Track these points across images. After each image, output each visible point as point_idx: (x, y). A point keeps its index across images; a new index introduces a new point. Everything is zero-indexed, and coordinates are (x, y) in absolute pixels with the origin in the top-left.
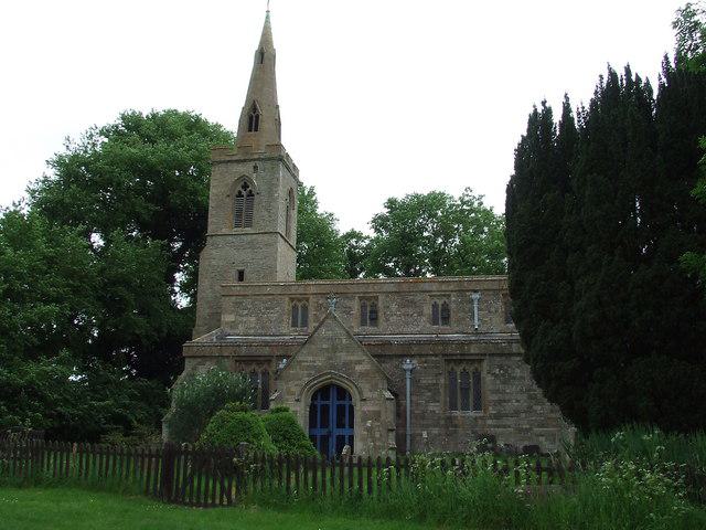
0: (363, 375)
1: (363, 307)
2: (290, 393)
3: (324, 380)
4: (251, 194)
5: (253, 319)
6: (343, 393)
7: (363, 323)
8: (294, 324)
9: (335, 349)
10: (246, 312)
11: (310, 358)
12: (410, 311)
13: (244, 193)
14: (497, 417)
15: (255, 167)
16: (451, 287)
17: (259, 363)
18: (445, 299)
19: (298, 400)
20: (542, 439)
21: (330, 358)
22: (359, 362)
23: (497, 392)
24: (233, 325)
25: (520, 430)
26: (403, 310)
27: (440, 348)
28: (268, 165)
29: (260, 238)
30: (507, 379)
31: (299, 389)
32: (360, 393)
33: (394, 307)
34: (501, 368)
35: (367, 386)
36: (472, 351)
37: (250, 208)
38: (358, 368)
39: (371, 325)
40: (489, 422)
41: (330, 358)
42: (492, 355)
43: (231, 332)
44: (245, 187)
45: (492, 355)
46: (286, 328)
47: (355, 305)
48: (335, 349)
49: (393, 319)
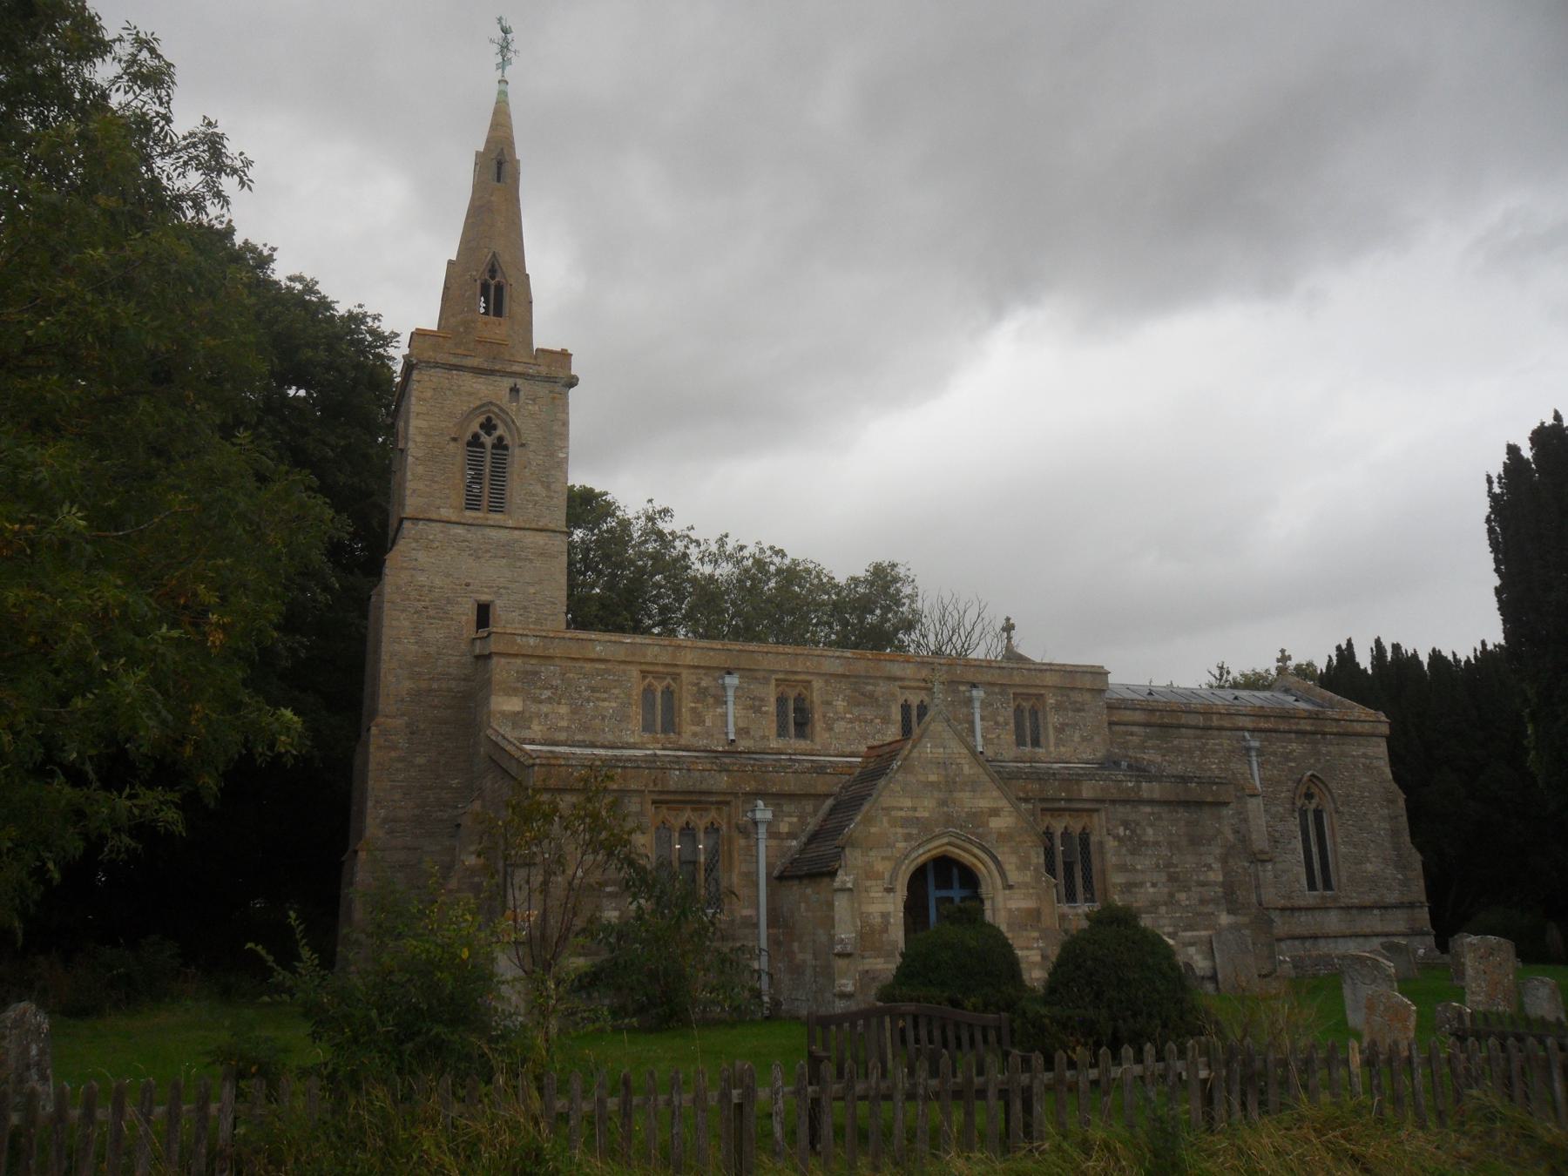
0: (1003, 837)
1: (781, 701)
2: (871, 874)
3: (922, 855)
4: (500, 444)
5: (563, 710)
6: (970, 879)
7: (782, 732)
8: (648, 727)
9: (950, 785)
10: (547, 693)
11: (908, 803)
12: (869, 713)
13: (487, 440)
15: (514, 390)
18: (923, 695)
19: (889, 890)
20: (1192, 950)
22: (995, 812)
23: (1123, 868)
24: (518, 719)
26: (856, 711)
27: (1036, 786)
28: (542, 390)
29: (531, 539)
30: (1135, 845)
31: (889, 865)
33: (840, 704)
34: (1126, 824)
36: (1085, 795)
38: (996, 823)
42: (1113, 802)
44: (488, 426)
45: (1113, 802)
46: (633, 731)
47: (771, 694)
49: (840, 726)
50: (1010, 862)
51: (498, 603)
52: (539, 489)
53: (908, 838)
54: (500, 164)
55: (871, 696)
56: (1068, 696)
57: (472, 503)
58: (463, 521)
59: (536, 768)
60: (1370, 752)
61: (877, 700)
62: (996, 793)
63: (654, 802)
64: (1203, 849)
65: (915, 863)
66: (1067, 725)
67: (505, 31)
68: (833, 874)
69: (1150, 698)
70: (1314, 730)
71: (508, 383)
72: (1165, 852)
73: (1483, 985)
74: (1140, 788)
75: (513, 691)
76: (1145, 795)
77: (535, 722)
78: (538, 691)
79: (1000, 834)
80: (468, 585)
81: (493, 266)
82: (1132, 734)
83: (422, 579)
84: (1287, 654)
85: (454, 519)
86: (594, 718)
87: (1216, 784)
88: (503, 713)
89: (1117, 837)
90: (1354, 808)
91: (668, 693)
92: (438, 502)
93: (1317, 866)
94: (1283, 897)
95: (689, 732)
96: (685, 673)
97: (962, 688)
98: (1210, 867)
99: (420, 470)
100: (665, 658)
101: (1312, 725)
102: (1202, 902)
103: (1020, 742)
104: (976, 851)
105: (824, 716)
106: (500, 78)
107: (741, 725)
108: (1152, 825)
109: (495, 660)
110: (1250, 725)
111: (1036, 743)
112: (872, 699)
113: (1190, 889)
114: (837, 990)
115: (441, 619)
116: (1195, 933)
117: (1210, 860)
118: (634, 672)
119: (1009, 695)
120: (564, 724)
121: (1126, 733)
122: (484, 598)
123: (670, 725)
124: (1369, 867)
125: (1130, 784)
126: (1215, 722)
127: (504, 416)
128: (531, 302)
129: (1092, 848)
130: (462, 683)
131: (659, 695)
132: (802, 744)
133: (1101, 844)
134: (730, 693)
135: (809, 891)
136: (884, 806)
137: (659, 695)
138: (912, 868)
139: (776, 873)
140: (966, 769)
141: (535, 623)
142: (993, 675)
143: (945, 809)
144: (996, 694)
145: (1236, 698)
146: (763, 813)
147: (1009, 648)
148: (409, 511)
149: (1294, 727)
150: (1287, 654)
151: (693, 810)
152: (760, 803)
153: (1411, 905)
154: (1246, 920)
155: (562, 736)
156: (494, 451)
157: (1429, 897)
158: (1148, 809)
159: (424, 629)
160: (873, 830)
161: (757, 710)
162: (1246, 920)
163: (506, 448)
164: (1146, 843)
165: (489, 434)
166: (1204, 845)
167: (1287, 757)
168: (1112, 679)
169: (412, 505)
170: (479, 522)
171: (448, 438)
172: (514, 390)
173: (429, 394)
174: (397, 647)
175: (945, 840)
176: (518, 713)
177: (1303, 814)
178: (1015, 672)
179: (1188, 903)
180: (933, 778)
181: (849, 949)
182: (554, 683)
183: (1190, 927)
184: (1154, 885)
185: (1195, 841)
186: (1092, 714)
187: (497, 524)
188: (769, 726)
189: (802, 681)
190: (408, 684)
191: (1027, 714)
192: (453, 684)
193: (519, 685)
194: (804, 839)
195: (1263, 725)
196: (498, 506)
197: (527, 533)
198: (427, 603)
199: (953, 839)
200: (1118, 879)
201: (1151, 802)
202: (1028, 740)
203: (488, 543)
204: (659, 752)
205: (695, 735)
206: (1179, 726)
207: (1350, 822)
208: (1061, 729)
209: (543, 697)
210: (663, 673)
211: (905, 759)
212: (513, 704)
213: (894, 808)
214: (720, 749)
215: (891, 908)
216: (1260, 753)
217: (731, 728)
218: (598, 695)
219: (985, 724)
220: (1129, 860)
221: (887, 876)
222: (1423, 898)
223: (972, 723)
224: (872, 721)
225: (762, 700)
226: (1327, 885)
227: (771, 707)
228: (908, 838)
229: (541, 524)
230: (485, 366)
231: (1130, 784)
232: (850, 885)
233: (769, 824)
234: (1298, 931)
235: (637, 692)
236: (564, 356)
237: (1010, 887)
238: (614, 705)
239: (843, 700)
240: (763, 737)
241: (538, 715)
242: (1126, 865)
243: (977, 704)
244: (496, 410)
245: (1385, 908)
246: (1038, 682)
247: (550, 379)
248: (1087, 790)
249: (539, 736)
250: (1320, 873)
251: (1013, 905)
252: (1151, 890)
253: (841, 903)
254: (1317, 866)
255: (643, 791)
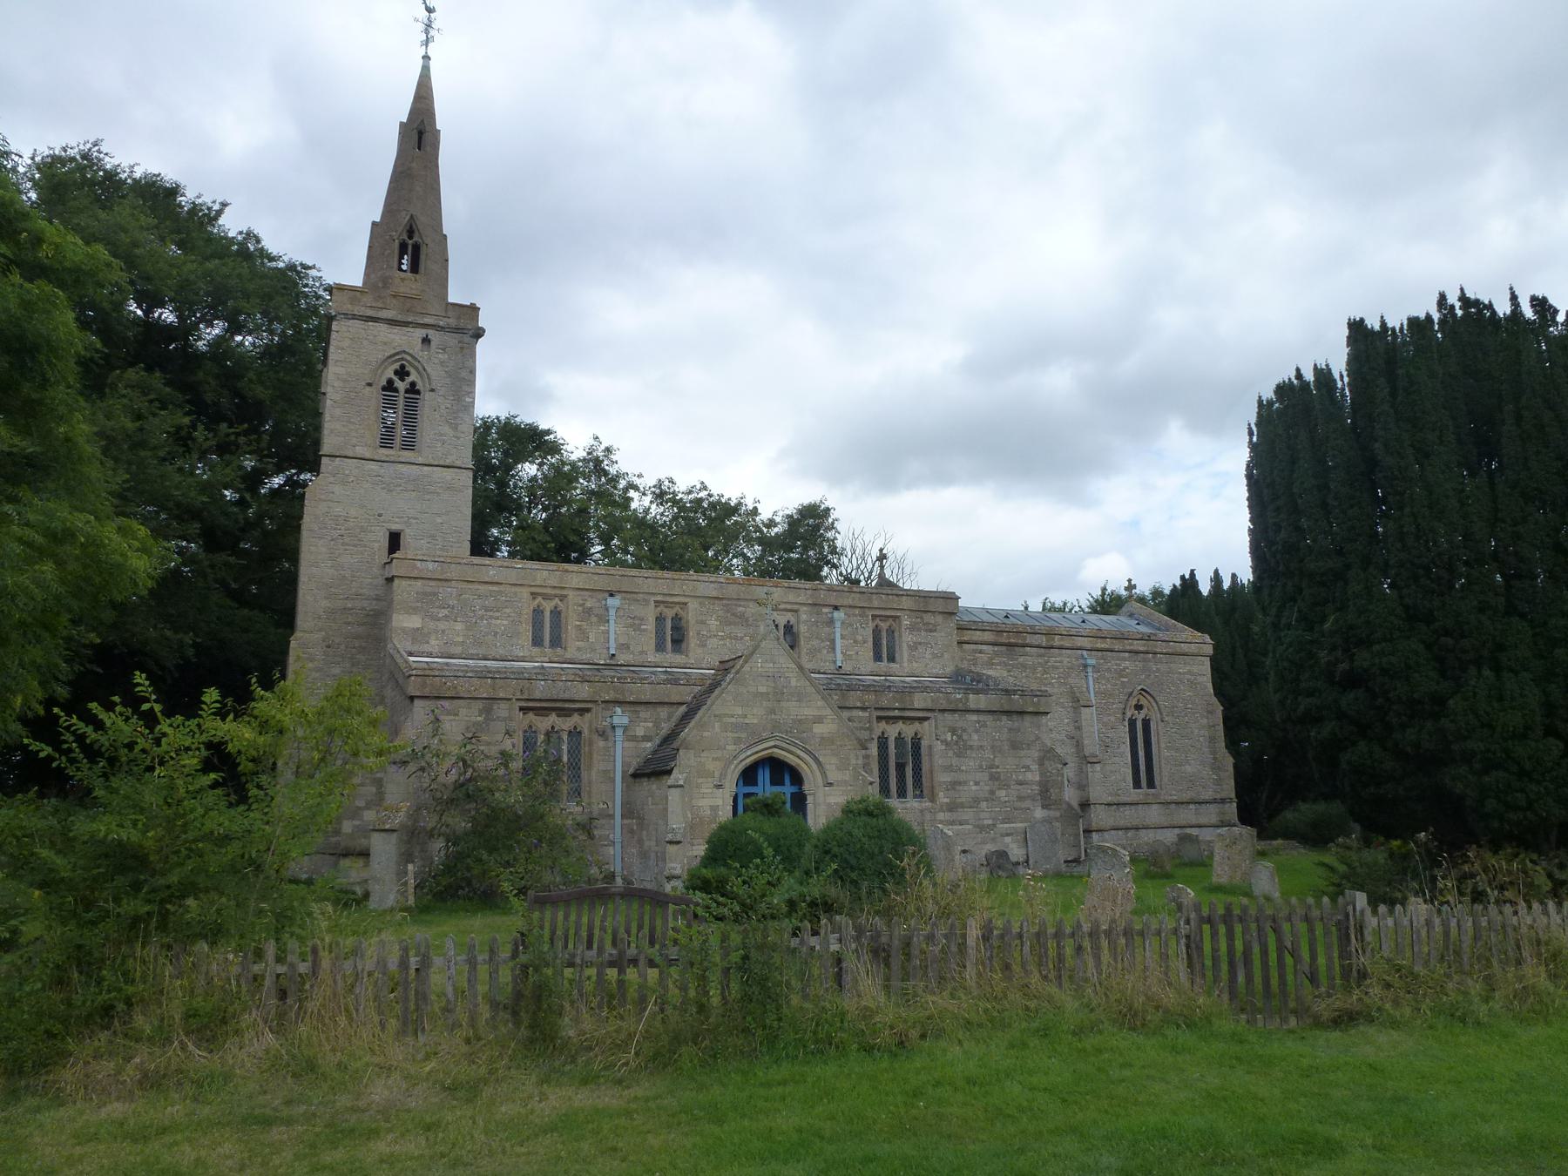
0: (826, 741)
1: (660, 619)
4: (413, 389)
7: (660, 647)
8: (537, 641)
9: (778, 695)
11: (739, 711)
13: (401, 386)
14: (952, 807)
15: (426, 341)
16: (801, 599)
17: (564, 713)
18: (790, 616)
19: (719, 787)
20: (1008, 840)
21: (773, 711)
22: (819, 720)
23: (948, 769)
24: (418, 635)
25: (982, 828)
26: (727, 629)
32: (824, 774)
33: (713, 623)
34: (953, 731)
35: (834, 760)
37: (411, 416)
38: (818, 729)
39: (674, 651)
40: (941, 816)
41: (773, 711)
42: (943, 711)
43: (415, 648)
44: (402, 373)
45: (943, 711)
46: (523, 645)
47: (650, 614)
48: (778, 695)
50: (831, 763)
51: (407, 531)
52: (447, 429)
53: (737, 741)
54: (421, 134)
55: (742, 616)
56: (922, 618)
57: (386, 441)
58: (376, 458)
59: (413, 678)
60: (1195, 669)
61: (747, 620)
62: (820, 703)
63: (521, 709)
64: (1022, 753)
65: (744, 763)
66: (920, 644)
67: (430, 10)
68: (669, 772)
69: (1006, 621)
70: (1145, 650)
71: (420, 333)
72: (988, 755)
73: (1226, 868)
74: (967, 699)
75: (415, 610)
76: (972, 706)
77: (433, 637)
78: (435, 610)
79: (822, 738)
80: (380, 515)
81: (411, 227)
82: (981, 652)
83: (338, 509)
84: (1133, 583)
85: (368, 455)
86: (487, 634)
87: (1036, 696)
88: (404, 630)
89: (945, 742)
90: (1178, 717)
91: (556, 613)
92: (354, 441)
93: (1143, 768)
94: (1110, 794)
95: (574, 647)
96: (571, 594)
97: (825, 610)
98: (1028, 768)
99: (338, 412)
100: (553, 582)
101: (1144, 646)
102: (1021, 798)
103: (878, 657)
104: (799, 752)
105: (698, 634)
106: (424, 53)
107: (621, 641)
108: (977, 731)
109: (396, 581)
110: (1089, 646)
111: (892, 659)
112: (743, 620)
113: (1009, 786)
114: (666, 873)
115: (355, 546)
116: (1012, 825)
117: (1028, 762)
118: (525, 593)
119: (867, 616)
120: (460, 639)
121: (975, 651)
122: (395, 527)
123: (556, 642)
124: (1188, 769)
125: (958, 696)
126: (1057, 641)
127: (416, 364)
128: (447, 260)
129: (924, 751)
130: (374, 602)
131: (547, 614)
132: (679, 659)
133: (930, 747)
134: (612, 612)
135: (654, 787)
136: (717, 713)
137: (547, 614)
138: (741, 767)
139: (631, 771)
140: (794, 682)
141: (441, 550)
142: (854, 599)
143: (773, 716)
144: (856, 616)
145: (1083, 622)
146: (620, 717)
147: (881, 576)
148: (325, 449)
149: (1128, 648)
150: (1133, 583)
151: (558, 716)
152: (619, 710)
153: (1223, 801)
154: (1058, 814)
155: (458, 650)
156: (407, 395)
157: (1237, 795)
158: (974, 717)
159: (339, 554)
160: (706, 734)
161: (637, 628)
162: (1058, 814)
163: (418, 392)
164: (971, 747)
165: (403, 380)
166: (1023, 749)
167: (1121, 673)
168: (961, 603)
169: (328, 444)
170: (392, 459)
171: (364, 383)
172: (426, 341)
173: (347, 343)
174: (314, 570)
175: (772, 743)
176: (418, 629)
177: (1132, 723)
178: (874, 597)
179: (1006, 799)
180: (762, 689)
181: (678, 838)
182: (451, 603)
183: (1007, 820)
184: (976, 783)
185: (1015, 746)
186: (943, 634)
187: (407, 460)
188: (650, 641)
189: (679, 603)
190: (325, 603)
191: (884, 634)
192: (365, 604)
193: (419, 604)
194: (657, 741)
195: (1100, 645)
196: (409, 445)
197: (435, 469)
198: (342, 532)
199: (778, 743)
200: (943, 778)
201: (978, 711)
202: (885, 656)
203: (400, 478)
204: (545, 665)
205: (579, 649)
206: (1024, 646)
207: (1173, 730)
208: (914, 647)
209: (440, 615)
210: (551, 595)
211: (737, 672)
212: (414, 622)
213: (725, 715)
214: (602, 662)
215: (720, 802)
216: (1096, 669)
217: (612, 644)
218: (491, 613)
219: (846, 642)
220: (955, 761)
221: (717, 774)
222: (1233, 795)
223: (833, 641)
224: (742, 638)
225: (642, 619)
226: (1151, 784)
227: (650, 626)
228: (737, 741)
229: (448, 462)
230: (399, 318)
231: (958, 696)
232: (681, 782)
233: (626, 729)
234: (1122, 823)
235: (527, 612)
236: (474, 309)
237: (831, 784)
238: (505, 622)
239: (716, 620)
240: (642, 652)
241: (436, 631)
242: (951, 765)
243: (838, 624)
244: (409, 358)
245: (1200, 803)
246: (895, 606)
247: (458, 330)
248: (919, 701)
249: (436, 650)
250: (1144, 773)
251: (832, 800)
252: (974, 788)
253: (674, 795)
254: (1143, 768)
255: (510, 699)
